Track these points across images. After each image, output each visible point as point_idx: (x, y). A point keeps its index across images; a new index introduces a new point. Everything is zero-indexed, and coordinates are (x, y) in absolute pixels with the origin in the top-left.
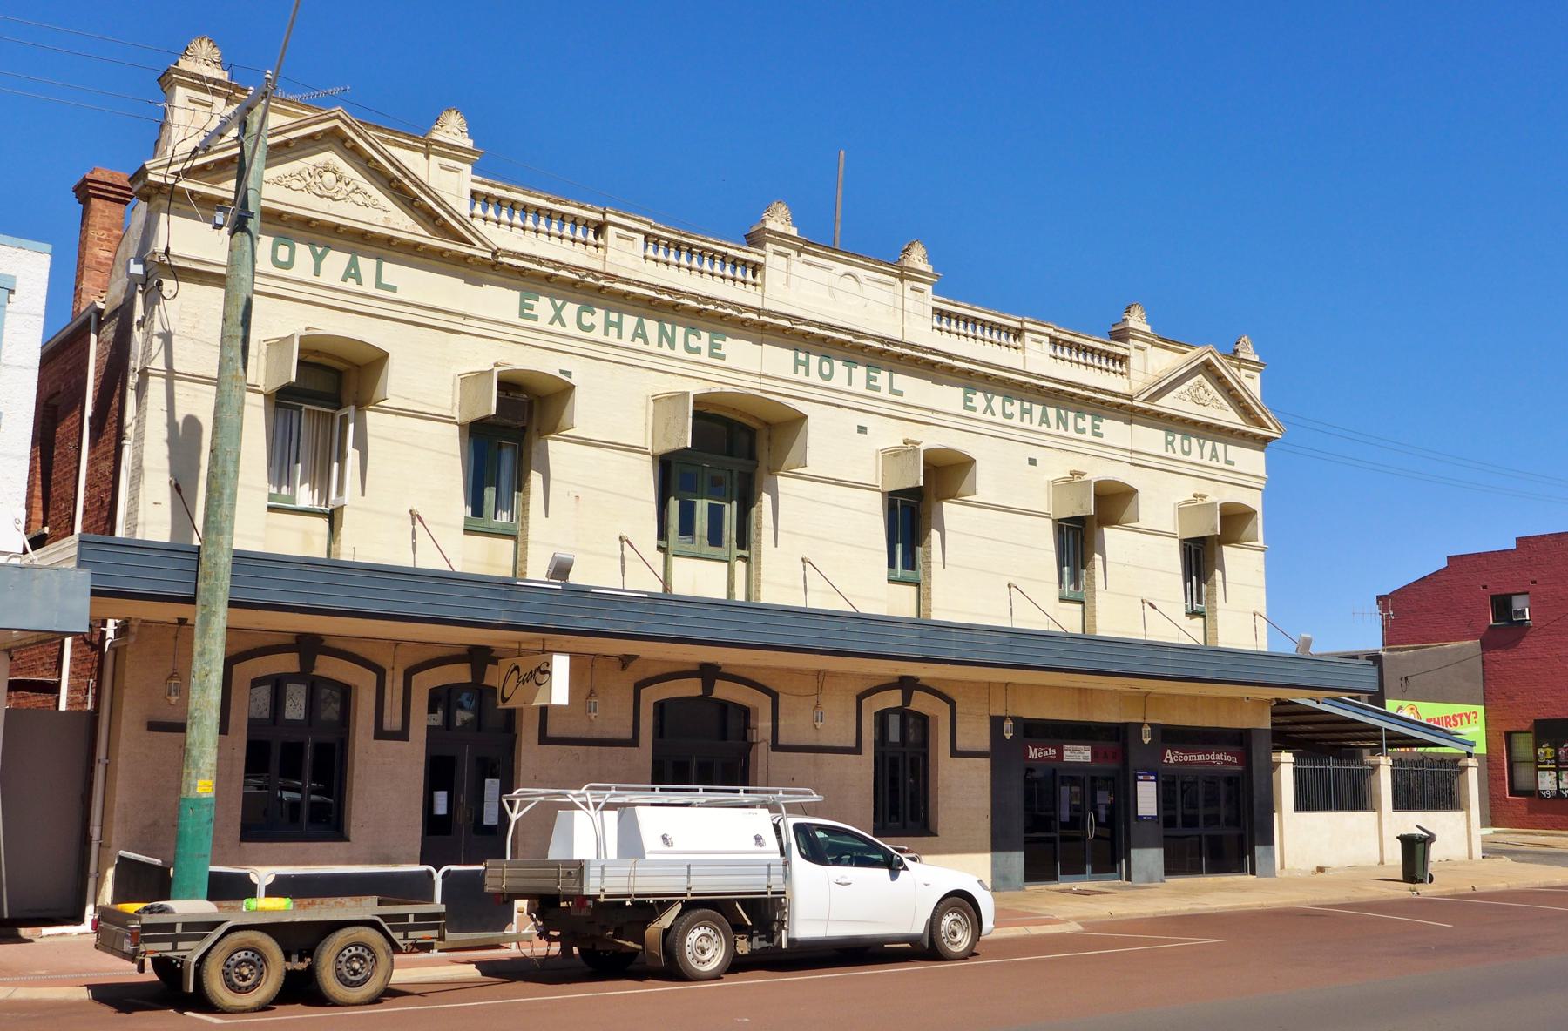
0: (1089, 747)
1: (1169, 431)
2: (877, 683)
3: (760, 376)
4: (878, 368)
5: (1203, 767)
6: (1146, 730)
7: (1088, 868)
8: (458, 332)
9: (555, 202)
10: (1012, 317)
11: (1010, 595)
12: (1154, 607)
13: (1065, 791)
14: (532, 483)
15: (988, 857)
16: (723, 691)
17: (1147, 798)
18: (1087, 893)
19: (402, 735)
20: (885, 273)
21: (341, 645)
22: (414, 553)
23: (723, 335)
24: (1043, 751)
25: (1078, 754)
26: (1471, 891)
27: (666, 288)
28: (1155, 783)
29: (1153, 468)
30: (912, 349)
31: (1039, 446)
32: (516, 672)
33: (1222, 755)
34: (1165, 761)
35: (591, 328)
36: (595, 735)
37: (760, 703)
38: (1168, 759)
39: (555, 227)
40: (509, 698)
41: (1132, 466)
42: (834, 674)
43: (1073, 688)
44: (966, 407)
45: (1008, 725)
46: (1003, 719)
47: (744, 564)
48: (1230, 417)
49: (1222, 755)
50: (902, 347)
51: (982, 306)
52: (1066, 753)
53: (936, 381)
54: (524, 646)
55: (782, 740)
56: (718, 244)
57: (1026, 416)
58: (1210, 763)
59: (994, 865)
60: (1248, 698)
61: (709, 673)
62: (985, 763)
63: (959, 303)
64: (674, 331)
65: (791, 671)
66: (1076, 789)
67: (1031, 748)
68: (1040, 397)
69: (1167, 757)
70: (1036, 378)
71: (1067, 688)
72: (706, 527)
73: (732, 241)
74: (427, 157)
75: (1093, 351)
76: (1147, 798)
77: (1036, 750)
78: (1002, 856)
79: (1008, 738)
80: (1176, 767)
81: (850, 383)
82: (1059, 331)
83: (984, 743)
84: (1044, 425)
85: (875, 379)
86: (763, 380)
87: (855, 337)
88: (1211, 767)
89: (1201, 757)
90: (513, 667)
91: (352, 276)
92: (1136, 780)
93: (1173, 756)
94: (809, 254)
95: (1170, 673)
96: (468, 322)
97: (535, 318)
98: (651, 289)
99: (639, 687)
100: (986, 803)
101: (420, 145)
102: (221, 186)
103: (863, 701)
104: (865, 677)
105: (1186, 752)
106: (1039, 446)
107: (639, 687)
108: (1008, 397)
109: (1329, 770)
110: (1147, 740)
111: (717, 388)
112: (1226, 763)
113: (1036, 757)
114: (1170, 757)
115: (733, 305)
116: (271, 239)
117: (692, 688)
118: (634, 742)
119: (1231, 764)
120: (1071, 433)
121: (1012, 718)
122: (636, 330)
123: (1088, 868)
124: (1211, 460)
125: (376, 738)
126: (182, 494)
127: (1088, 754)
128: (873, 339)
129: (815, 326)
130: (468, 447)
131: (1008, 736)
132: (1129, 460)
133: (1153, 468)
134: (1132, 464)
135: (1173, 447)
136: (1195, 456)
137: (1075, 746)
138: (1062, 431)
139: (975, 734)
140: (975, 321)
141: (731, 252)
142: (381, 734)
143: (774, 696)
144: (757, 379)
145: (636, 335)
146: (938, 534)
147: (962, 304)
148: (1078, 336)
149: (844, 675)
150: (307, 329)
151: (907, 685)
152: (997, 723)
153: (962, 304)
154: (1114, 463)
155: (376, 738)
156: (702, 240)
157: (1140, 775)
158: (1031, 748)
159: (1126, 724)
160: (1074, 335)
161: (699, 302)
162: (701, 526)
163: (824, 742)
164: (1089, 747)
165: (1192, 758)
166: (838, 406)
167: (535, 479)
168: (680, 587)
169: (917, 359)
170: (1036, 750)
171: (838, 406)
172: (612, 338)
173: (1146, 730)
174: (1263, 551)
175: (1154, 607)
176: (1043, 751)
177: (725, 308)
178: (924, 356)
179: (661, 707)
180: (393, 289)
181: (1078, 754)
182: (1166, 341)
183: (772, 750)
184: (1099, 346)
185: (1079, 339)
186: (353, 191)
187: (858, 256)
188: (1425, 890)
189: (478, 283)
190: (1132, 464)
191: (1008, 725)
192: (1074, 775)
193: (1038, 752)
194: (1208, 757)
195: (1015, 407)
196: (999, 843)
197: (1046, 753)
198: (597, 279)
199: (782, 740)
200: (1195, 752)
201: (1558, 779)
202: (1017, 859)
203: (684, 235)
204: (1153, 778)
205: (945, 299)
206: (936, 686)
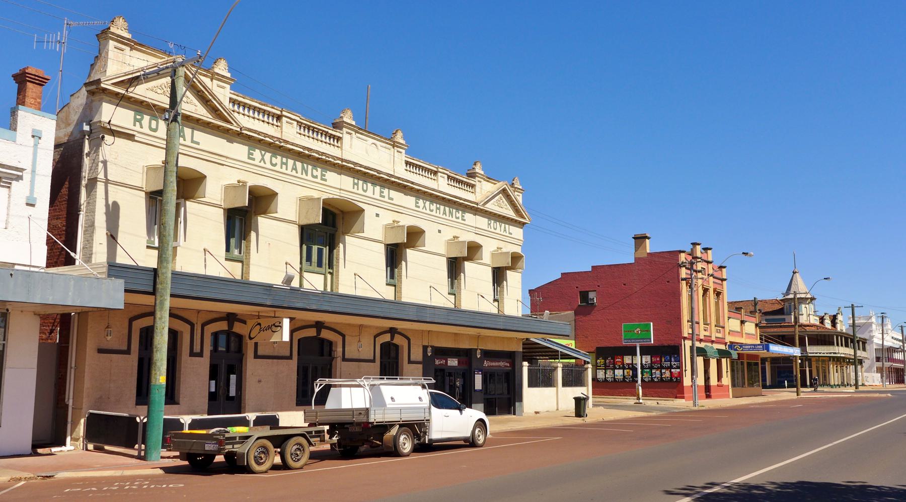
0: (457, 359)
1: (489, 219)
3: (340, 189)
6: (479, 351)
8: (223, 165)
12: (483, 297)
19: (200, 355)
20: (387, 143)
25: (453, 362)
32: (258, 326)
35: (275, 165)
36: (276, 354)
42: (366, 327)
45: (429, 349)
48: (510, 213)
56: (325, 128)
58: (500, 366)
61: (319, 326)
62: (420, 366)
65: (349, 325)
70: (444, 194)
71: (450, 333)
81: (374, 194)
86: (342, 192)
87: (378, 173)
88: (500, 368)
89: (497, 364)
90: (257, 323)
92: (474, 374)
97: (254, 159)
98: (301, 148)
101: (209, 75)
104: (377, 328)
110: (479, 356)
111: (331, 196)
117: (312, 332)
119: (507, 366)
121: (431, 346)
122: (293, 166)
127: (457, 362)
128: (384, 175)
132: (474, 231)
134: (475, 233)
139: (417, 354)
141: (330, 132)
142: (192, 354)
143: (343, 336)
144: (338, 191)
145: (293, 169)
146: (405, 263)
152: (425, 348)
156: (319, 126)
161: (319, 155)
163: (362, 357)
164: (457, 359)
165: (494, 364)
166: (369, 204)
168: (307, 286)
169: (399, 184)
171: (369, 204)
173: (479, 351)
175: (483, 297)
177: (329, 158)
178: (403, 183)
180: (198, 143)
181: (453, 362)
182: (489, 178)
187: (378, 136)
190: (475, 233)
191: (429, 349)
197: (441, 362)
198: (280, 142)
200: (495, 361)
201: (605, 373)
203: (312, 123)
204: (480, 373)
205: (409, 157)
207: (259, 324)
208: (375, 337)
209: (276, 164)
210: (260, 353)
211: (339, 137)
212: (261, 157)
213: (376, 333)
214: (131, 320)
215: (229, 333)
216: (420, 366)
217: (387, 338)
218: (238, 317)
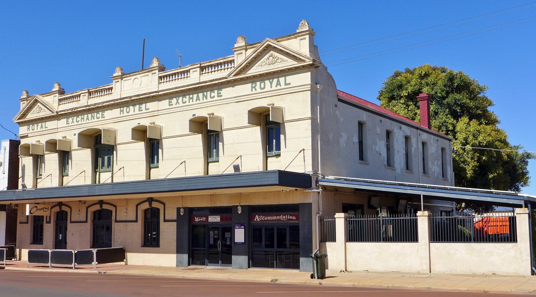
1: (252, 82)
2: (143, 200)
4: (142, 104)
5: (275, 222)
6: (240, 209)
7: (220, 262)
9: (72, 94)
10: (185, 67)
11: (185, 165)
13: (211, 233)
14: (69, 161)
15: (175, 255)
16: (105, 207)
17: (240, 235)
18: (194, 269)
20: (145, 73)
21: (156, 199)
22: (304, 162)
23: (220, 89)
24: (200, 219)
25: (215, 219)
26: (387, 288)
27: (222, 78)
28: (244, 229)
29: (247, 100)
30: (145, 95)
31: (197, 109)
33: (286, 216)
34: (255, 220)
36: (80, 220)
37: (112, 209)
38: (257, 219)
39: (223, 67)
40: (33, 213)
41: (114, 123)
42: (131, 199)
43: (208, 195)
44: (170, 105)
45: (182, 210)
46: (181, 208)
47: (64, 177)
48: (291, 63)
49: (286, 216)
50: (142, 95)
51: (174, 69)
52: (209, 219)
53: (233, 86)
54: (45, 202)
55: (135, 219)
56: (103, 87)
57: (122, 112)
58: (279, 220)
59: (177, 258)
60: (283, 191)
62: (175, 223)
63: (167, 71)
64: (207, 94)
65: (120, 200)
66: (216, 232)
67: (196, 218)
68: (196, 91)
69: (256, 218)
70: (187, 86)
71: (206, 195)
72: (107, 163)
73: (105, 84)
74: (296, 39)
75: (221, 64)
76: (240, 235)
77: (198, 218)
78: (180, 255)
79: (182, 215)
82: (203, 63)
83: (175, 217)
84: (198, 101)
85: (103, 115)
89: (274, 218)
92: (235, 228)
93: (259, 218)
94: (125, 78)
95: (167, 190)
96: (159, 112)
98: (84, 107)
100: (175, 237)
102: (26, 118)
103: (139, 206)
104: (139, 199)
105: (266, 216)
106: (197, 109)
107: (87, 208)
108: (184, 96)
109: (380, 220)
110: (239, 212)
111: (82, 130)
112: (290, 220)
113: (198, 221)
114: (258, 218)
115: (100, 103)
116: (217, 91)
118: (86, 222)
119: (292, 220)
120: (96, 120)
121: (183, 208)
122: (87, 118)
123: (220, 262)
124: (41, 129)
125: (137, 222)
128: (134, 97)
129: (119, 100)
131: (182, 214)
133: (247, 100)
134: (236, 102)
135: (29, 130)
136: (131, 112)
138: (205, 100)
139: (172, 214)
140: (175, 74)
141: (106, 87)
142: (47, 223)
143: (116, 207)
146: (161, 150)
147: (168, 71)
148: (212, 62)
149: (133, 199)
150: (138, 124)
151: (150, 200)
152: (178, 209)
153: (168, 71)
154: (228, 104)
155: (137, 222)
156: (100, 88)
157: (237, 226)
158: (196, 218)
160: (210, 62)
161: (94, 106)
162: (106, 164)
163: (128, 219)
165: (270, 218)
166: (132, 119)
167: (70, 161)
169: (147, 97)
170: (198, 218)
171: (132, 119)
172: (205, 100)
173: (240, 209)
174: (310, 119)
176: (200, 219)
177: (99, 105)
178: (149, 95)
181: (215, 219)
182: (252, 45)
184: (221, 61)
185: (212, 62)
186: (277, 60)
187: (136, 72)
188: (325, 282)
189: (161, 100)
190: (236, 102)
191: (182, 210)
192: (214, 226)
193: (199, 219)
194: (278, 217)
195: (186, 99)
196: (179, 251)
197: (201, 219)
198: (74, 110)
199: (118, 219)
200: (272, 216)
202: (185, 257)
203: (96, 88)
204: (243, 227)
205: (170, 71)
206: (159, 199)
207: (36, 207)
208: (137, 206)
209: (79, 121)
211: (111, 88)
216: (175, 223)
217: (146, 206)
218: (63, 203)
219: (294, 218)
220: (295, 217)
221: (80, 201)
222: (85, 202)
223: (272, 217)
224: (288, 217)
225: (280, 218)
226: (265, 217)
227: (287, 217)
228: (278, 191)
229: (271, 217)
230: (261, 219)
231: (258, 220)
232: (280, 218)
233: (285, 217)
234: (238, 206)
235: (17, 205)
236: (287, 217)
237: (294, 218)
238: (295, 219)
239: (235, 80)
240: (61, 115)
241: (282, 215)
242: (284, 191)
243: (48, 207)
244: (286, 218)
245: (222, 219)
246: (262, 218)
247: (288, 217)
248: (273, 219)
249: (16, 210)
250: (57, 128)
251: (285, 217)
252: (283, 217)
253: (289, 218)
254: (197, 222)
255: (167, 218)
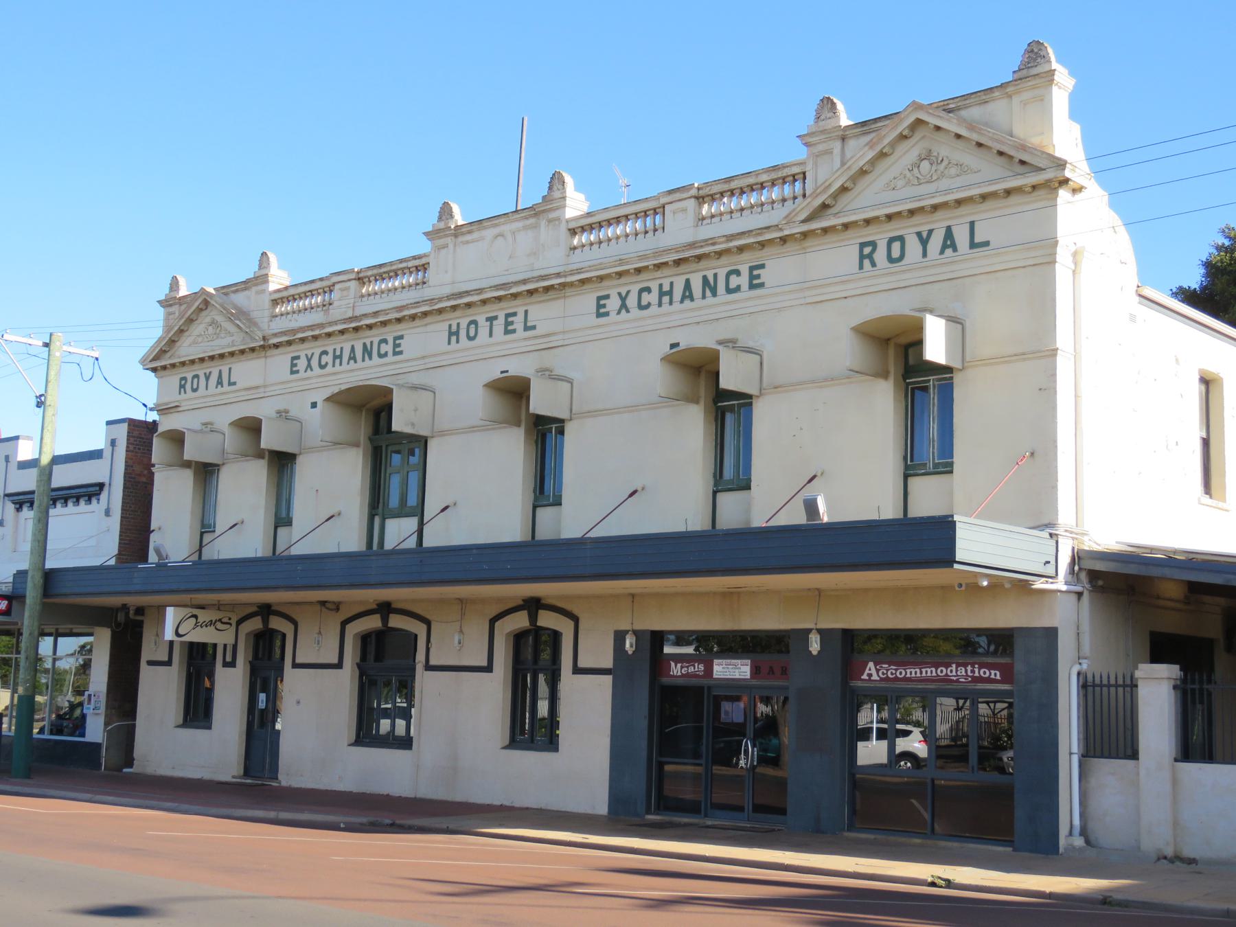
0: (749, 662)
3: (423, 357)
16: (396, 622)
24: (688, 667)
33: (969, 668)
34: (865, 677)
37: (419, 629)
38: (870, 675)
46: (627, 632)
49: (969, 668)
54: (221, 603)
61: (385, 609)
62: (608, 679)
67: (673, 664)
69: (867, 671)
77: (679, 665)
80: (883, 685)
86: (427, 360)
88: (959, 686)
91: (687, 297)
93: (878, 671)
99: (344, 624)
104: (499, 600)
107: (344, 624)
113: (679, 674)
114: (873, 672)
119: (989, 680)
122: (350, 354)
126: (808, 485)
130: (895, 399)
132: (802, 301)
137: (729, 661)
139: (597, 651)
145: (350, 358)
152: (620, 637)
158: (673, 664)
159: (793, 630)
164: (749, 662)
170: (679, 665)
176: (688, 667)
179: (365, 639)
183: (426, 670)
193: (682, 667)
194: (942, 671)
197: (691, 669)
207: (195, 616)
208: (492, 622)
209: (327, 363)
210: (581, 664)
211: (423, 265)
212: (620, 302)
213: (494, 614)
214: (492, 622)
215: (536, 631)
216: (608, 679)
217: (520, 621)
219: (995, 675)
220: (998, 673)
221: (323, 603)
222: (337, 607)
223: (920, 669)
224: (976, 670)
225: (947, 675)
226: (896, 670)
227: (973, 671)
228: (943, 587)
229: (918, 671)
230: (883, 674)
231: (875, 677)
232: (947, 675)
233: (966, 671)
234: (809, 631)
235: (140, 610)
236: (973, 671)
237: (995, 675)
238: (998, 677)
239: (805, 235)
240: (276, 346)
241: (954, 666)
242: (964, 585)
243: (230, 619)
244: (967, 675)
245: (756, 671)
246: (887, 670)
247: (976, 670)
248: (924, 674)
249: (140, 624)
250: (265, 386)
251: (966, 671)
252: (957, 671)
253: (977, 674)
254: (676, 677)
255: (582, 664)
